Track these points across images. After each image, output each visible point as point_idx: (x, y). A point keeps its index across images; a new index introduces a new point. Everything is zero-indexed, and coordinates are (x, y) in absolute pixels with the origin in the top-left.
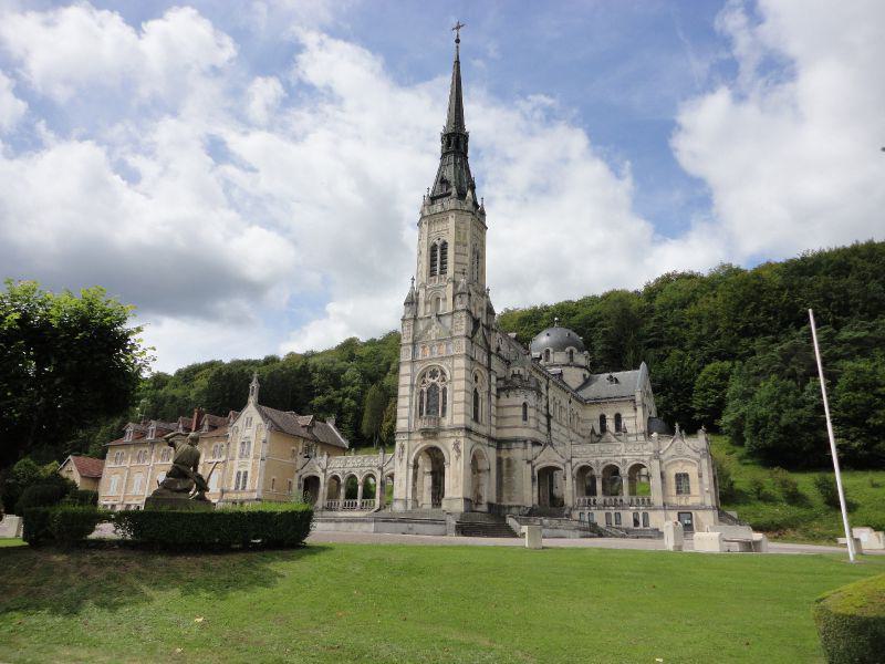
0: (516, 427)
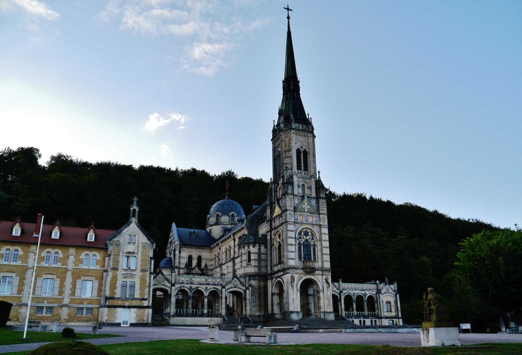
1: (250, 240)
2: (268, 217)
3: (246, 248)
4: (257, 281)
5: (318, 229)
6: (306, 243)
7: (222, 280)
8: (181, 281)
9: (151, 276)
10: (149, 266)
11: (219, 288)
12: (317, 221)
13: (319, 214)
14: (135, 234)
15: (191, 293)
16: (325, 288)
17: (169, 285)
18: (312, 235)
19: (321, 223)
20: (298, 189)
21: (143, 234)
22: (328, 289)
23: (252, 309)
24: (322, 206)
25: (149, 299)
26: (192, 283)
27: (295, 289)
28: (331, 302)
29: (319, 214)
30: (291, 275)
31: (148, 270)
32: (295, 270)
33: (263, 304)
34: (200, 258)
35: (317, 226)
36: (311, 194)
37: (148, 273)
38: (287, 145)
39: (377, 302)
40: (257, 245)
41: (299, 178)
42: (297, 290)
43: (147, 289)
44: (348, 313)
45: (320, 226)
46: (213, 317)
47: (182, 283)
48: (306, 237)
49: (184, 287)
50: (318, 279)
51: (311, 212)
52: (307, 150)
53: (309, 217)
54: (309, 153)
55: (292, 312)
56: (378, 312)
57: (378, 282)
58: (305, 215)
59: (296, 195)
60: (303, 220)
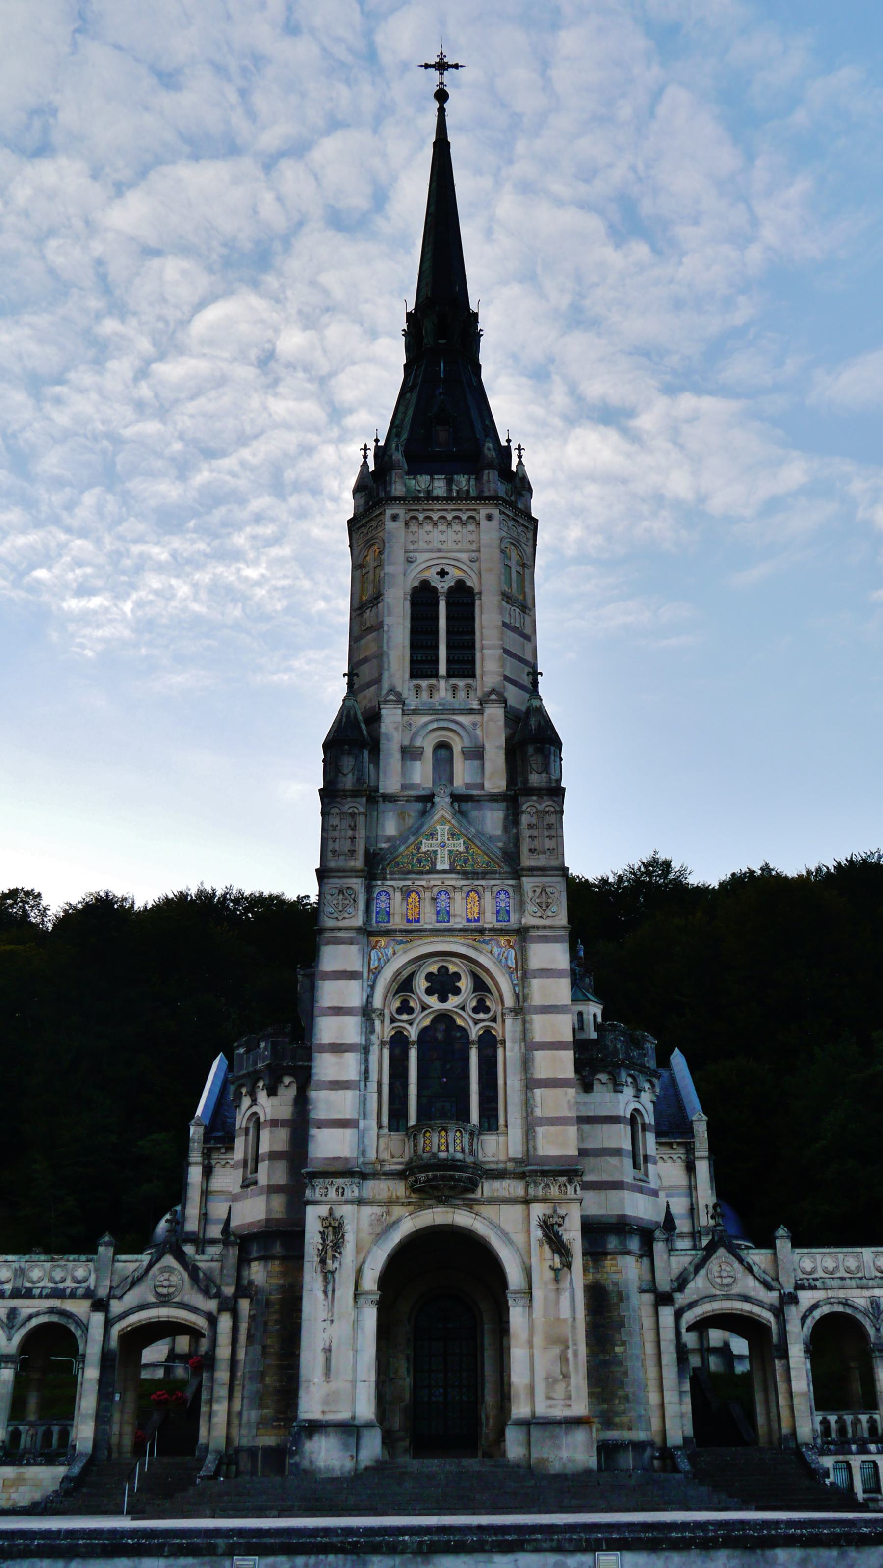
0: (618, 1185)
5: (512, 952)
6: (440, 1036)
12: (508, 912)
13: (517, 873)
18: (480, 986)
19: (529, 920)
20: (403, 766)
22: (557, 1280)
23: (245, 1414)
24: (535, 833)
27: (345, 1292)
29: (517, 873)
30: (323, 1210)
32: (347, 1181)
35: (503, 940)
36: (479, 781)
40: (287, 1080)
41: (415, 712)
42: (357, 1294)
44: (841, 1422)
45: (522, 934)
48: (443, 999)
50: (497, 1227)
51: (469, 869)
52: (469, 584)
53: (458, 896)
54: (480, 593)
58: (436, 890)
59: (390, 798)
60: (422, 916)
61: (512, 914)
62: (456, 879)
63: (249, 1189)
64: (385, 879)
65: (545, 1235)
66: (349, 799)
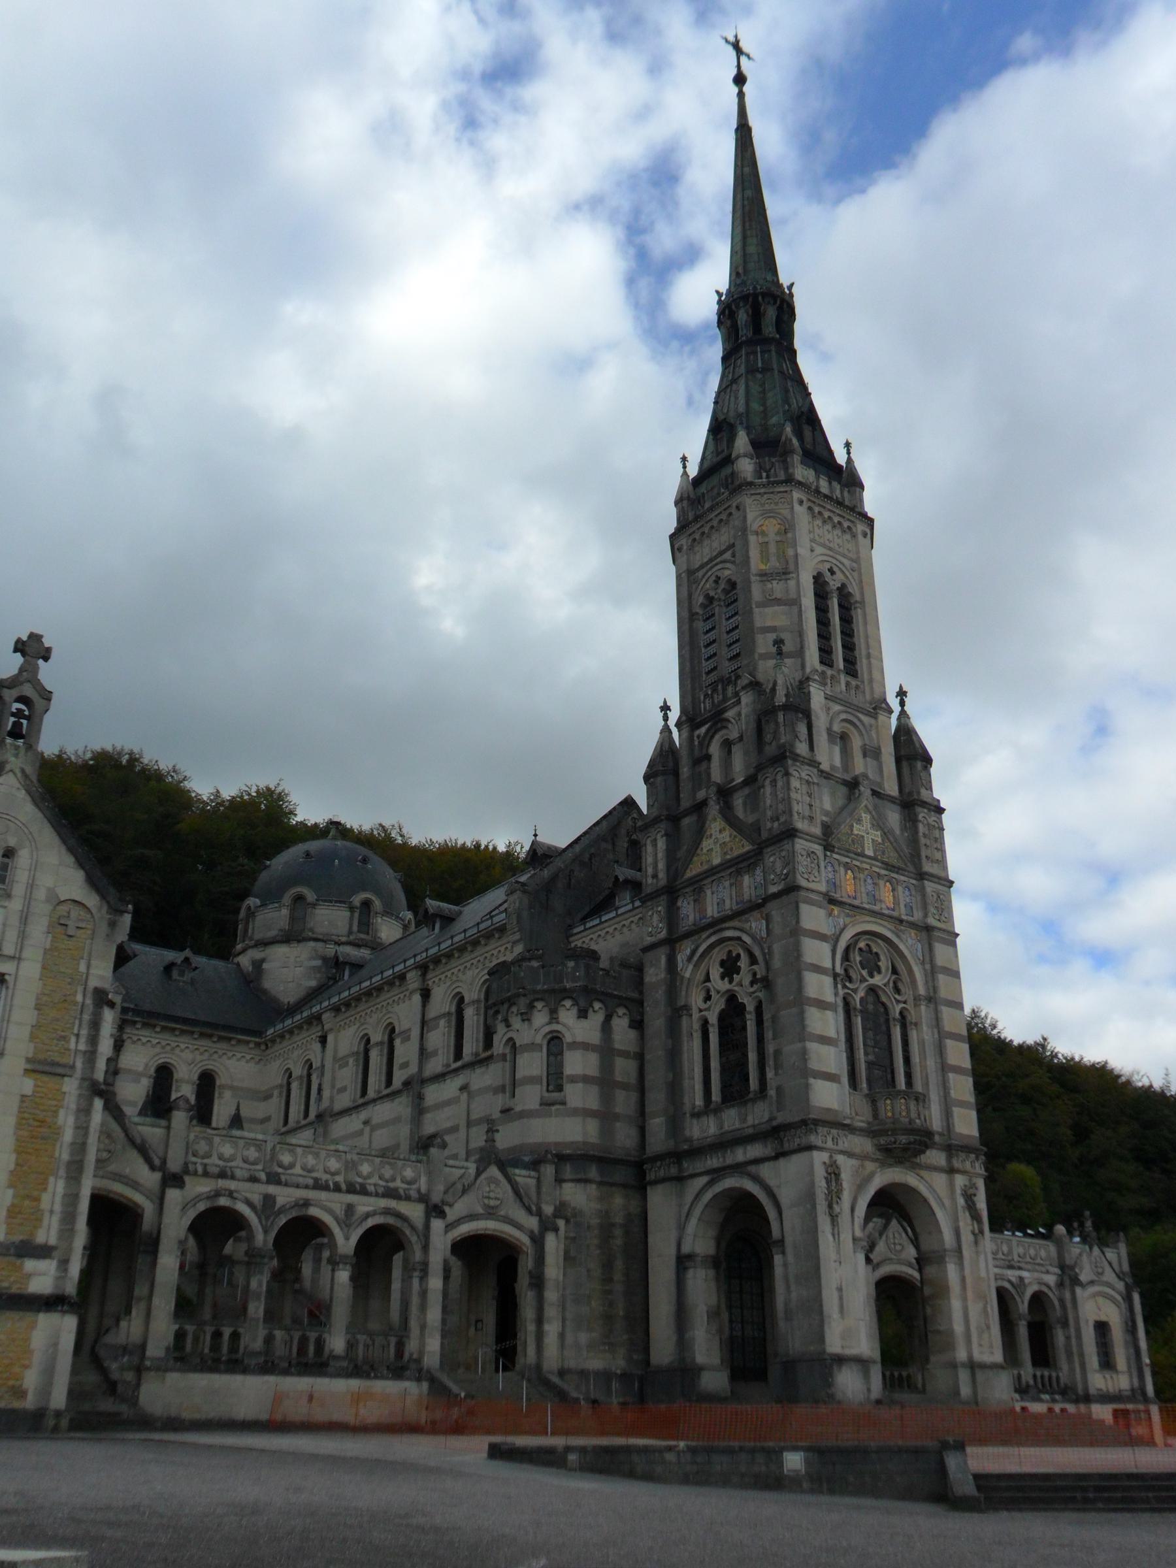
1: (562, 982)
2: (655, 876)
3: (540, 1018)
4: (592, 1189)
7: (429, 1174)
8: (214, 1160)
9: (91, 1104)
10: (83, 1040)
11: (415, 1212)
14: (12, 842)
15: (266, 1232)
16: (967, 1238)
17: (150, 1179)
19: (931, 921)
21: (63, 849)
22: (976, 1243)
23: (569, 1339)
25: (69, 1250)
26: (274, 1179)
27: (846, 1237)
28: (992, 1307)
31: (73, 1067)
33: (621, 1313)
34: (207, 1083)
37: (71, 1087)
38: (772, 548)
39: (1065, 1324)
40: (597, 1005)
43: (58, 1187)
46: (376, 1377)
47: (222, 1175)
49: (231, 1194)
53: (881, 883)
55: (840, 1360)
56: (1072, 1370)
57: (1060, 1229)
61: (915, 911)
62: (880, 868)
63: (553, 1108)
64: (832, 851)
65: (966, 1201)
66: (807, 767)
